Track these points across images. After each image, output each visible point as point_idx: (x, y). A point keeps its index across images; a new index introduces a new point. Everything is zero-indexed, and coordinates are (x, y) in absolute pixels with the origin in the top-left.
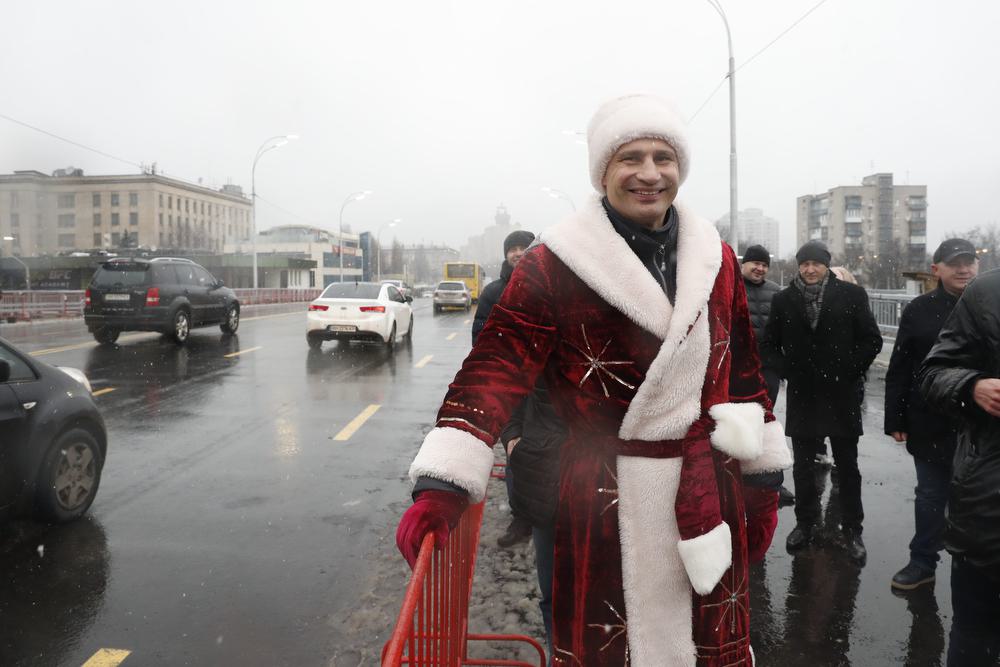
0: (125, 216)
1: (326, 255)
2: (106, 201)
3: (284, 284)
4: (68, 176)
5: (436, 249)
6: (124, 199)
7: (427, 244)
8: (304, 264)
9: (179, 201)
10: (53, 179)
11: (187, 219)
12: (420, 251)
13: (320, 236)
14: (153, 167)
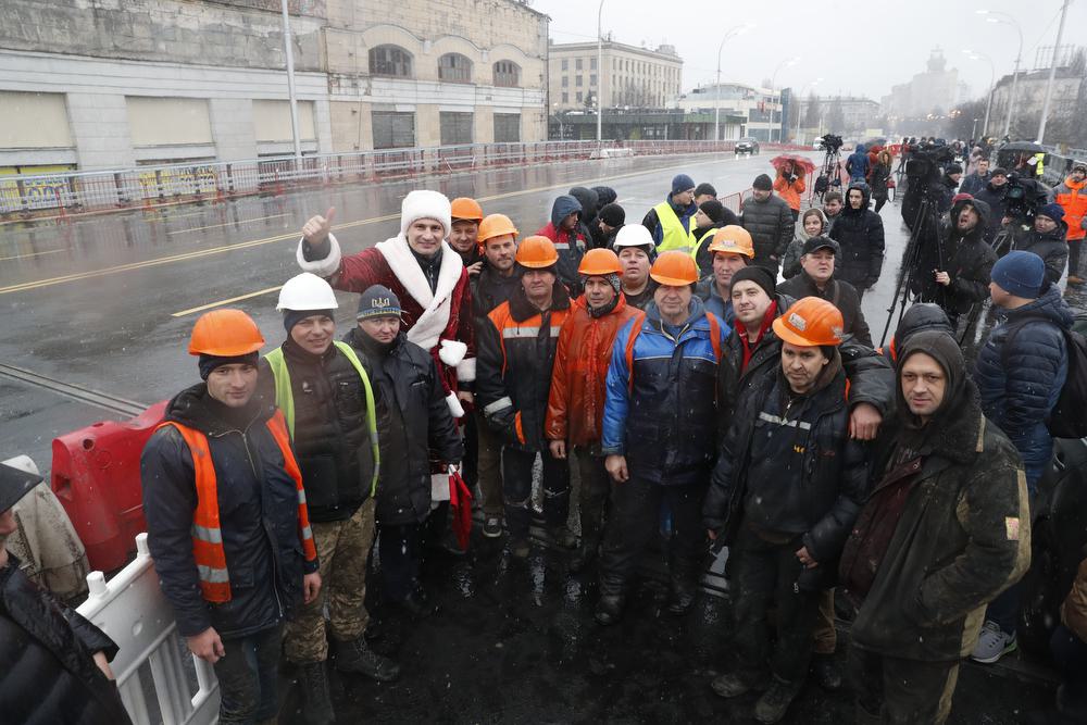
0: (586, 76)
1: (751, 110)
3: (721, 137)
5: (853, 100)
6: (586, 63)
7: (844, 95)
8: (734, 120)
11: (633, 79)
12: (837, 102)
13: (746, 92)
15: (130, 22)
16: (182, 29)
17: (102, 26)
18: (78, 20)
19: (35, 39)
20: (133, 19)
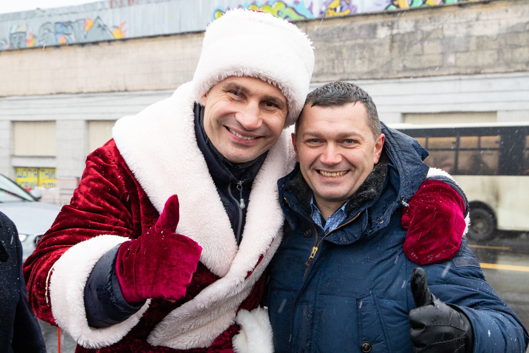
15: (422, 41)
16: (478, 37)
17: (396, 51)
18: (377, 49)
19: (341, 71)
20: (426, 37)
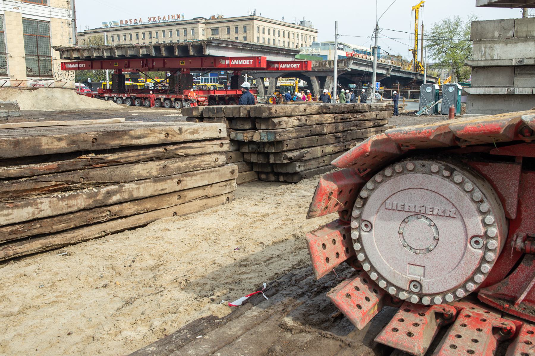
2: (233, 30)
4: (216, 19)
9: (269, 29)
10: (210, 21)
14: (254, 11)
